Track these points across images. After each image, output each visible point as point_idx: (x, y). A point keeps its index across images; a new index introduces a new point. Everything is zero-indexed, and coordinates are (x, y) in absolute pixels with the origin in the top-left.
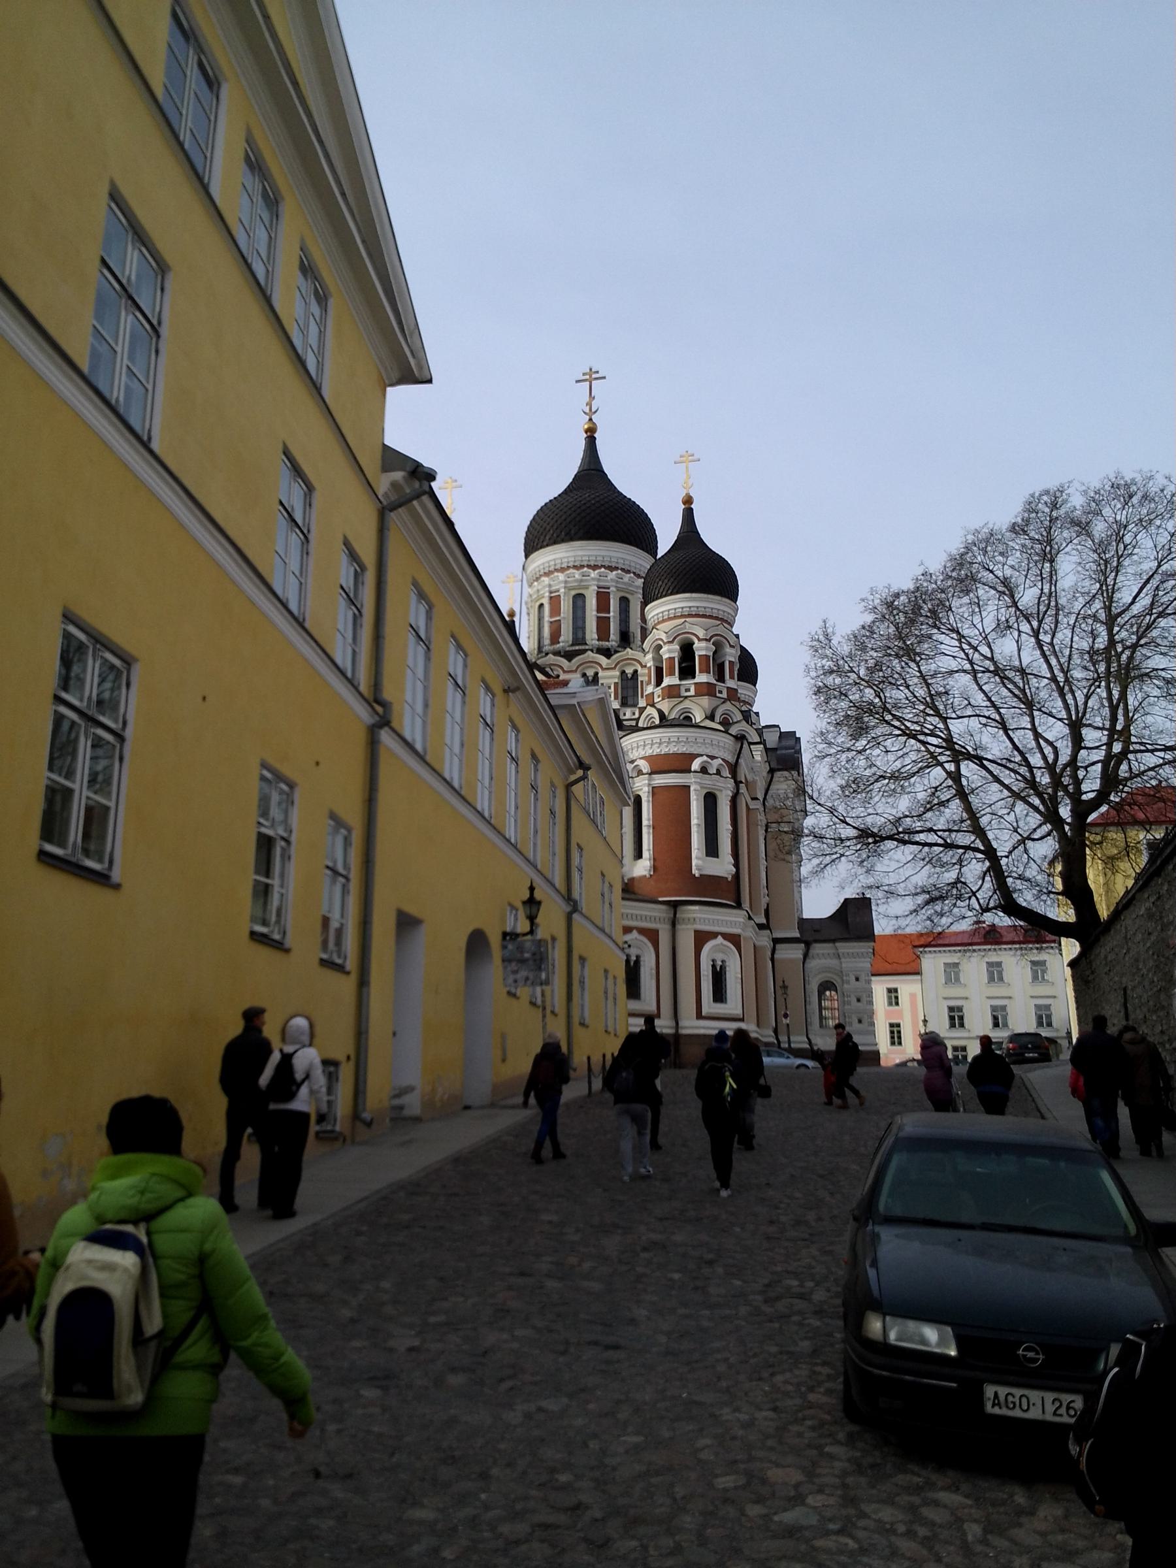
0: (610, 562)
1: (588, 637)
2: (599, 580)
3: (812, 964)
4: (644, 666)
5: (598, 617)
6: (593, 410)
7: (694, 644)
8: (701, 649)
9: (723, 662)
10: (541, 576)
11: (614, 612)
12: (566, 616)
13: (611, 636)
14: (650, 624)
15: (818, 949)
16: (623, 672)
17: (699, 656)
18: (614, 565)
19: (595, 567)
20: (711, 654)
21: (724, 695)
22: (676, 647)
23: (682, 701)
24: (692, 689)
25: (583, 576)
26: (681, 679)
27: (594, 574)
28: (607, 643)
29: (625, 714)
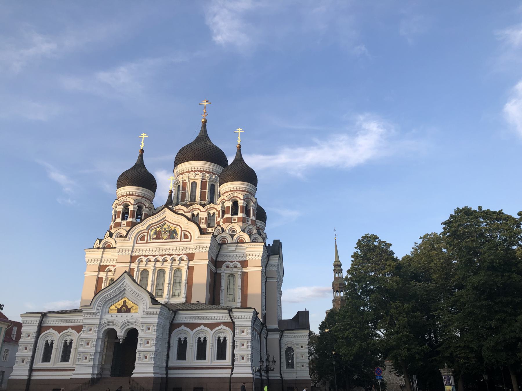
1: (196, 199)
3: (285, 340)
4: (217, 211)
5: (201, 191)
6: (206, 114)
7: (238, 201)
8: (241, 203)
9: (250, 210)
11: (208, 189)
15: (286, 333)
16: (209, 213)
17: (240, 206)
20: (245, 205)
25: (196, 175)
26: (232, 215)
27: (200, 174)
28: (204, 202)
29: (209, 230)
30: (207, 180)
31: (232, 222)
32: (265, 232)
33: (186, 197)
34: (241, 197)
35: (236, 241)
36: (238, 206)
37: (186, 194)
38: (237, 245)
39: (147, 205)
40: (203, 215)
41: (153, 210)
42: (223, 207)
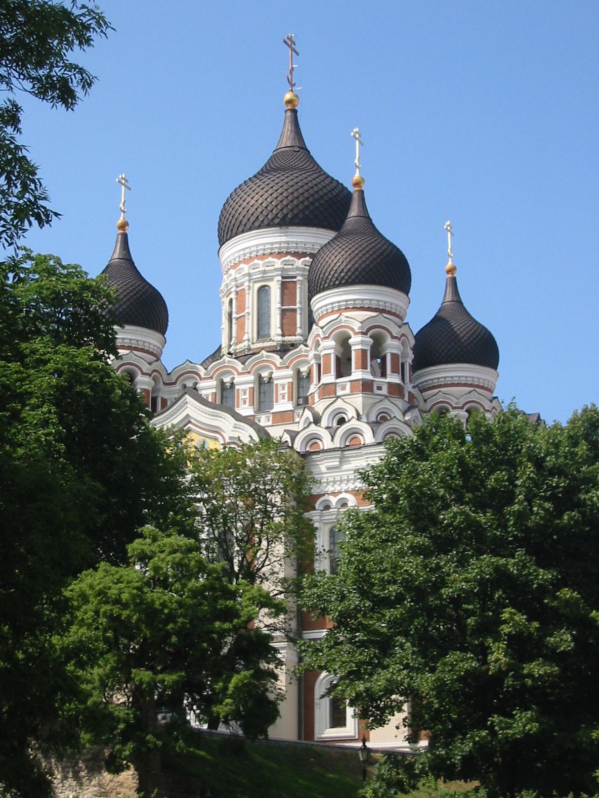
0: (297, 247)
2: (283, 270)
7: (350, 338)
8: (357, 342)
10: (229, 269)
11: (300, 303)
12: (250, 311)
13: (298, 329)
14: (316, 316)
17: (355, 350)
18: (300, 251)
19: (280, 254)
20: (368, 348)
21: (384, 391)
22: (331, 343)
23: (335, 401)
24: (348, 386)
26: (339, 375)
27: (278, 263)
30: (295, 277)
31: (338, 394)
32: (494, 395)
33: (246, 331)
34: (356, 326)
35: (340, 444)
36: (351, 351)
37: (247, 321)
38: (342, 454)
39: (146, 368)
40: (283, 377)
41: (165, 377)
42: (317, 357)
